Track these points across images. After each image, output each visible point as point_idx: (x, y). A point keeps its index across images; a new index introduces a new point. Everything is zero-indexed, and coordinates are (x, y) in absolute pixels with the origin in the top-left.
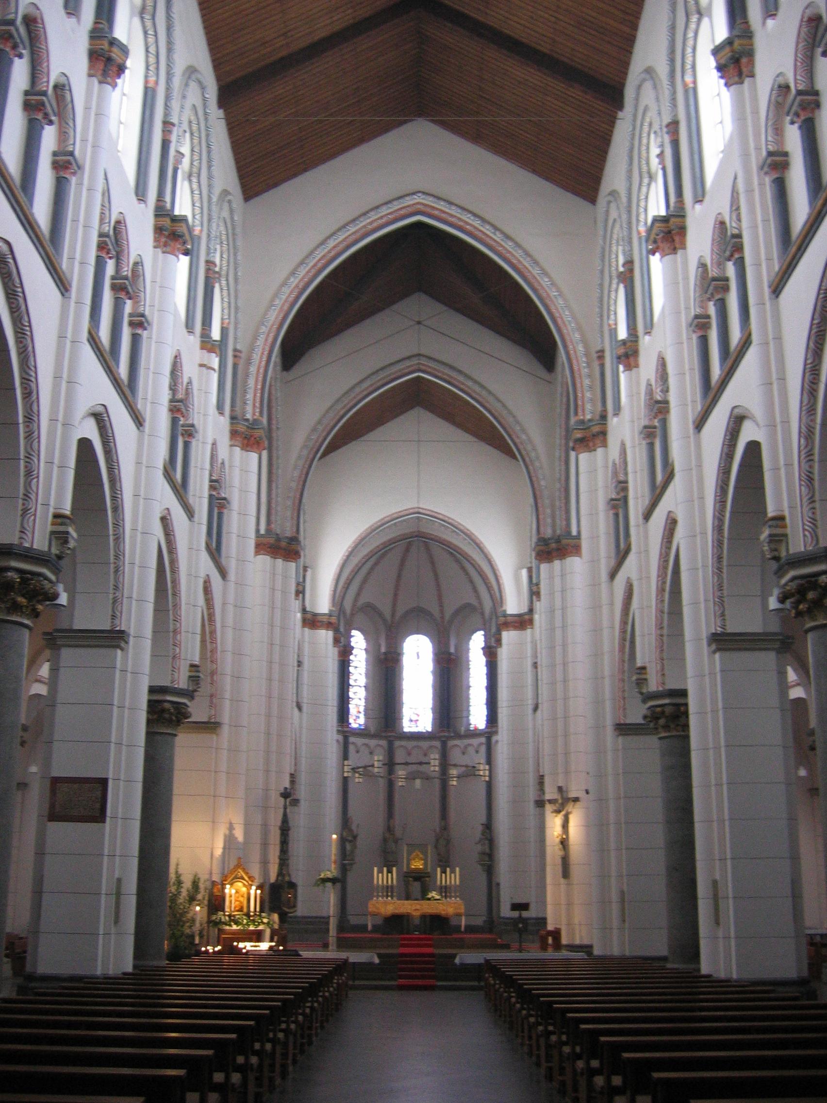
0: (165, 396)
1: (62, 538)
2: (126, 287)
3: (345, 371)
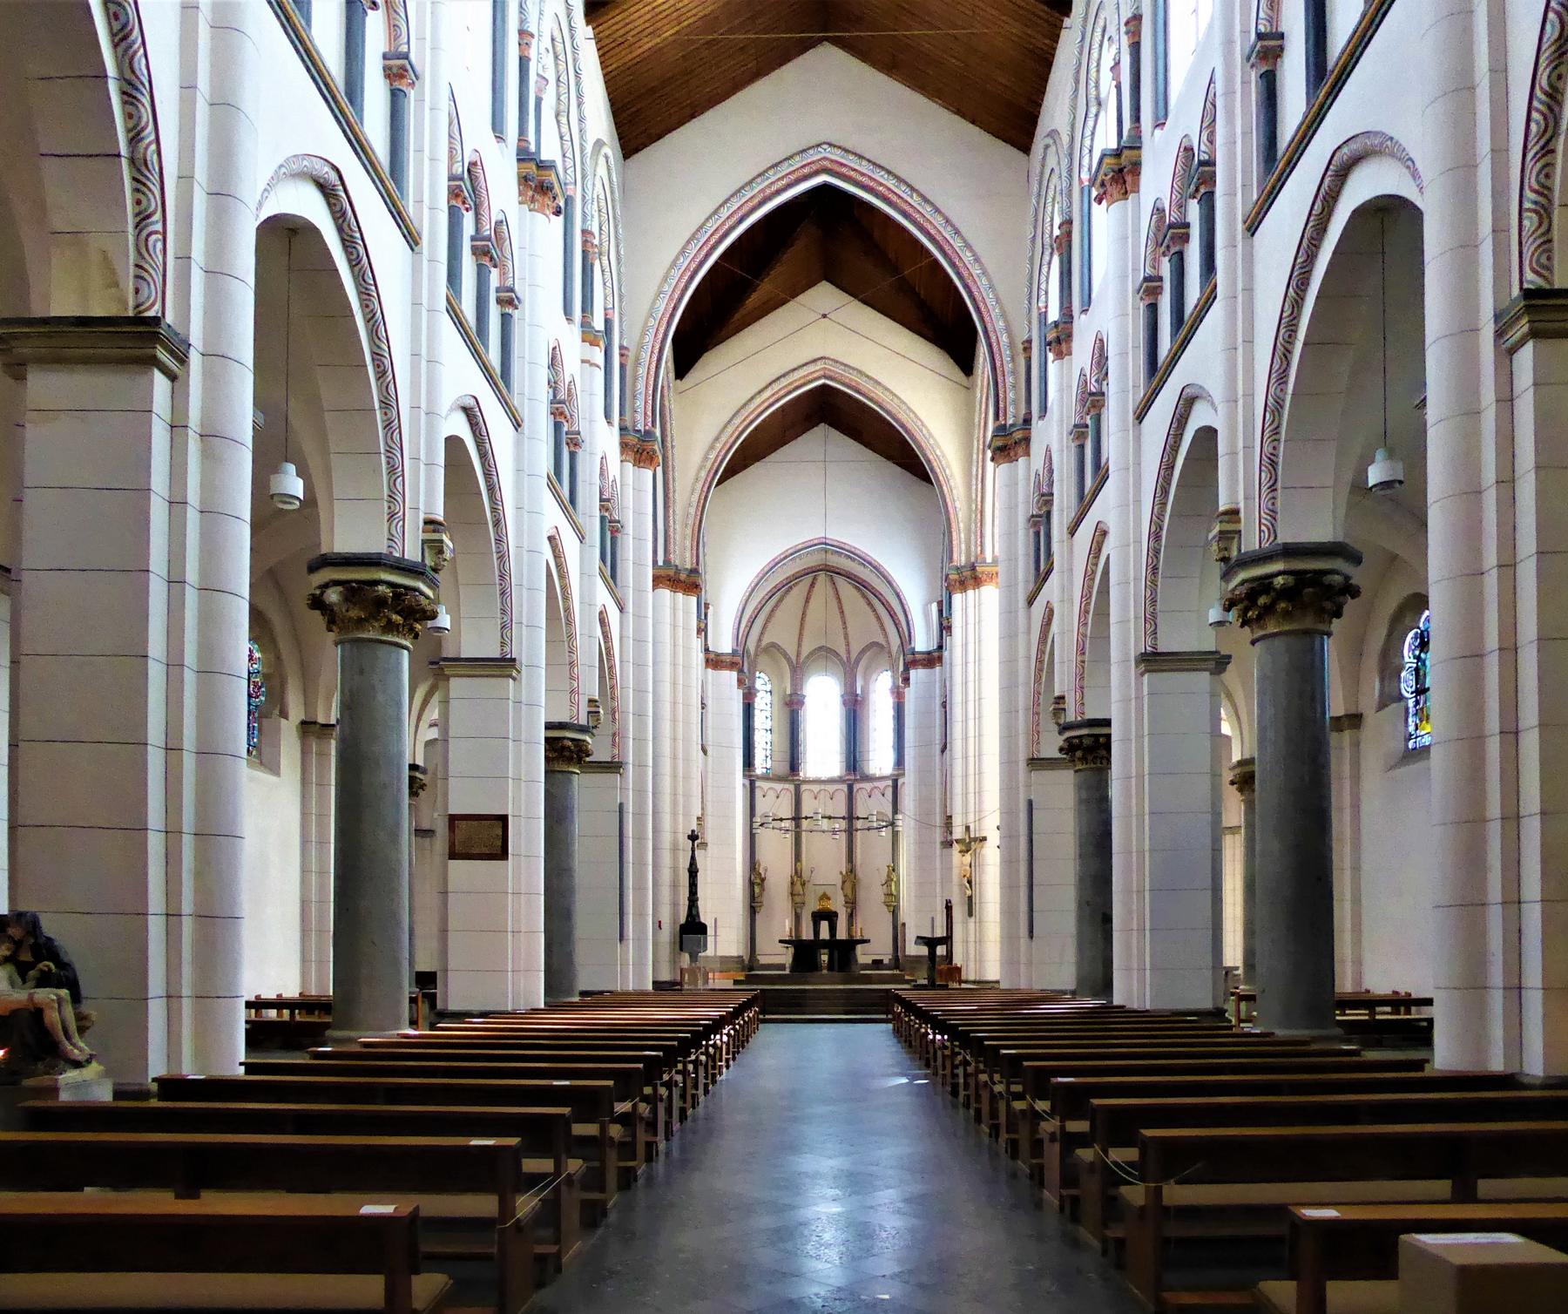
0: (544, 394)
2: (489, 251)
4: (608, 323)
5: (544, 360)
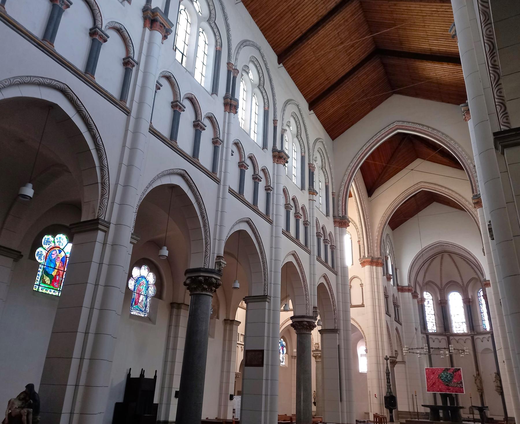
1: (219, 264)
3: (394, 193)
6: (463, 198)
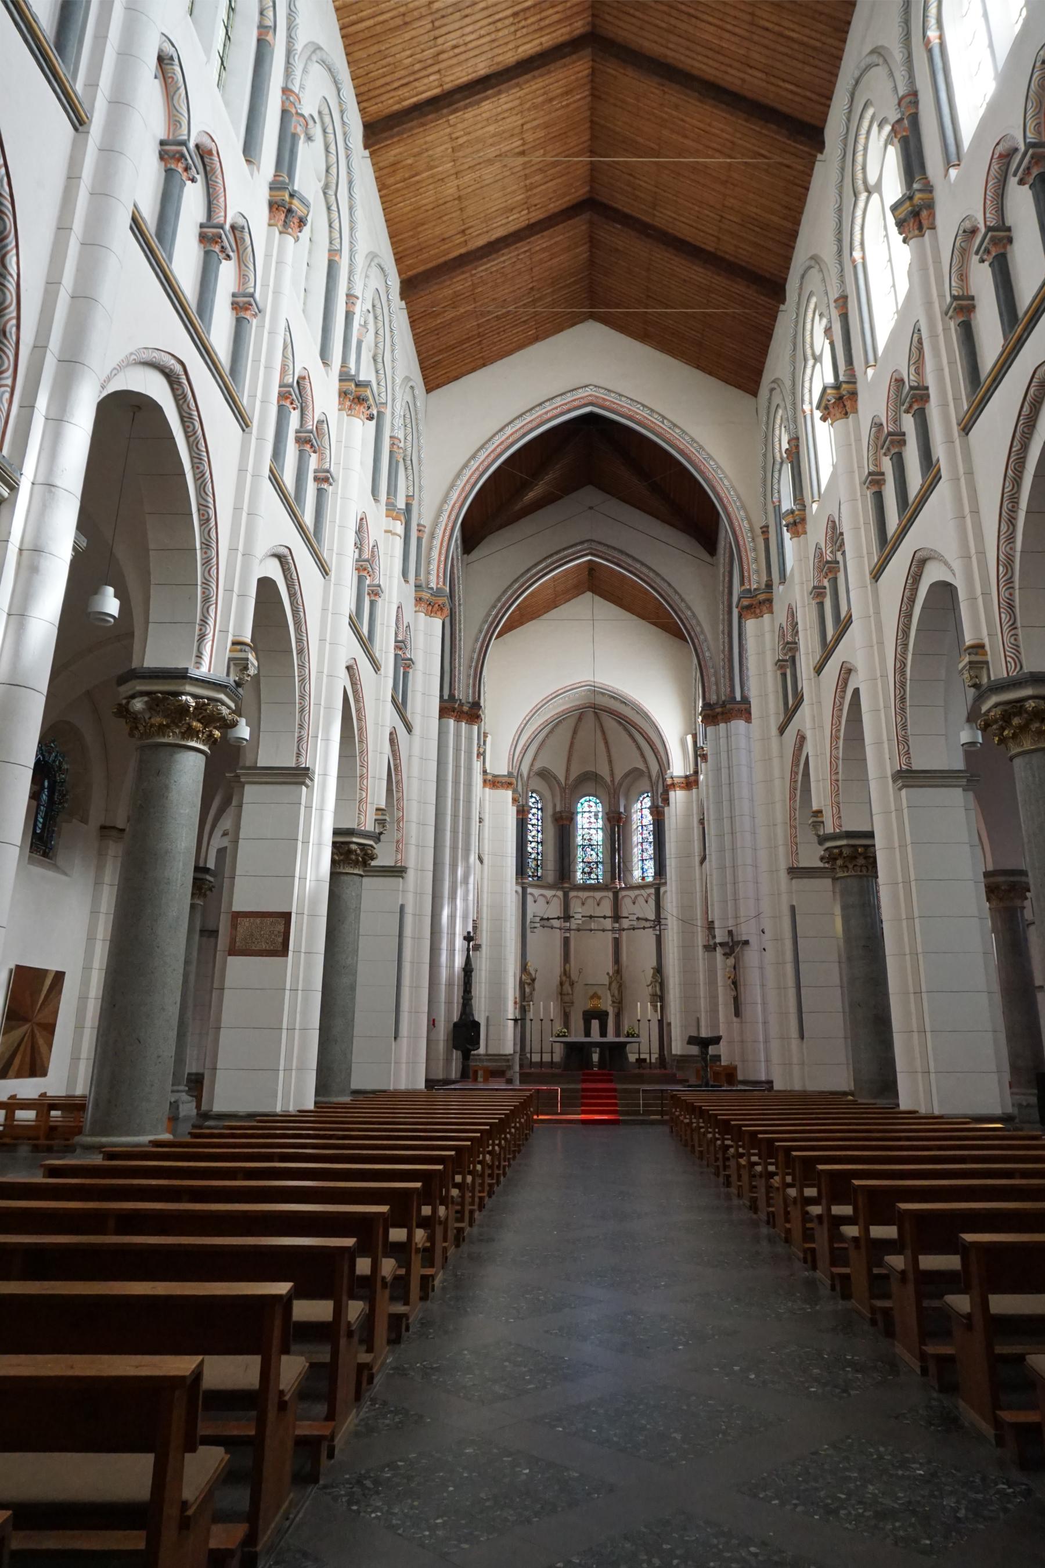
0: (350, 555)
4: (408, 506)
5: (352, 526)
6: (676, 592)
